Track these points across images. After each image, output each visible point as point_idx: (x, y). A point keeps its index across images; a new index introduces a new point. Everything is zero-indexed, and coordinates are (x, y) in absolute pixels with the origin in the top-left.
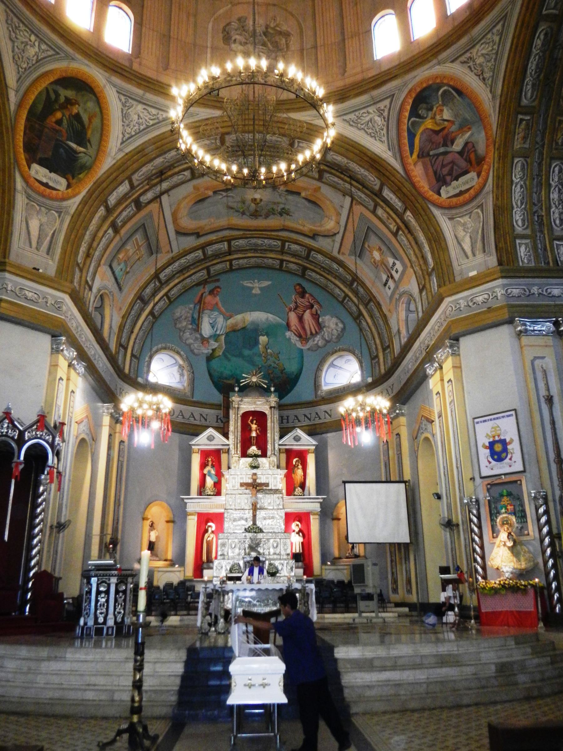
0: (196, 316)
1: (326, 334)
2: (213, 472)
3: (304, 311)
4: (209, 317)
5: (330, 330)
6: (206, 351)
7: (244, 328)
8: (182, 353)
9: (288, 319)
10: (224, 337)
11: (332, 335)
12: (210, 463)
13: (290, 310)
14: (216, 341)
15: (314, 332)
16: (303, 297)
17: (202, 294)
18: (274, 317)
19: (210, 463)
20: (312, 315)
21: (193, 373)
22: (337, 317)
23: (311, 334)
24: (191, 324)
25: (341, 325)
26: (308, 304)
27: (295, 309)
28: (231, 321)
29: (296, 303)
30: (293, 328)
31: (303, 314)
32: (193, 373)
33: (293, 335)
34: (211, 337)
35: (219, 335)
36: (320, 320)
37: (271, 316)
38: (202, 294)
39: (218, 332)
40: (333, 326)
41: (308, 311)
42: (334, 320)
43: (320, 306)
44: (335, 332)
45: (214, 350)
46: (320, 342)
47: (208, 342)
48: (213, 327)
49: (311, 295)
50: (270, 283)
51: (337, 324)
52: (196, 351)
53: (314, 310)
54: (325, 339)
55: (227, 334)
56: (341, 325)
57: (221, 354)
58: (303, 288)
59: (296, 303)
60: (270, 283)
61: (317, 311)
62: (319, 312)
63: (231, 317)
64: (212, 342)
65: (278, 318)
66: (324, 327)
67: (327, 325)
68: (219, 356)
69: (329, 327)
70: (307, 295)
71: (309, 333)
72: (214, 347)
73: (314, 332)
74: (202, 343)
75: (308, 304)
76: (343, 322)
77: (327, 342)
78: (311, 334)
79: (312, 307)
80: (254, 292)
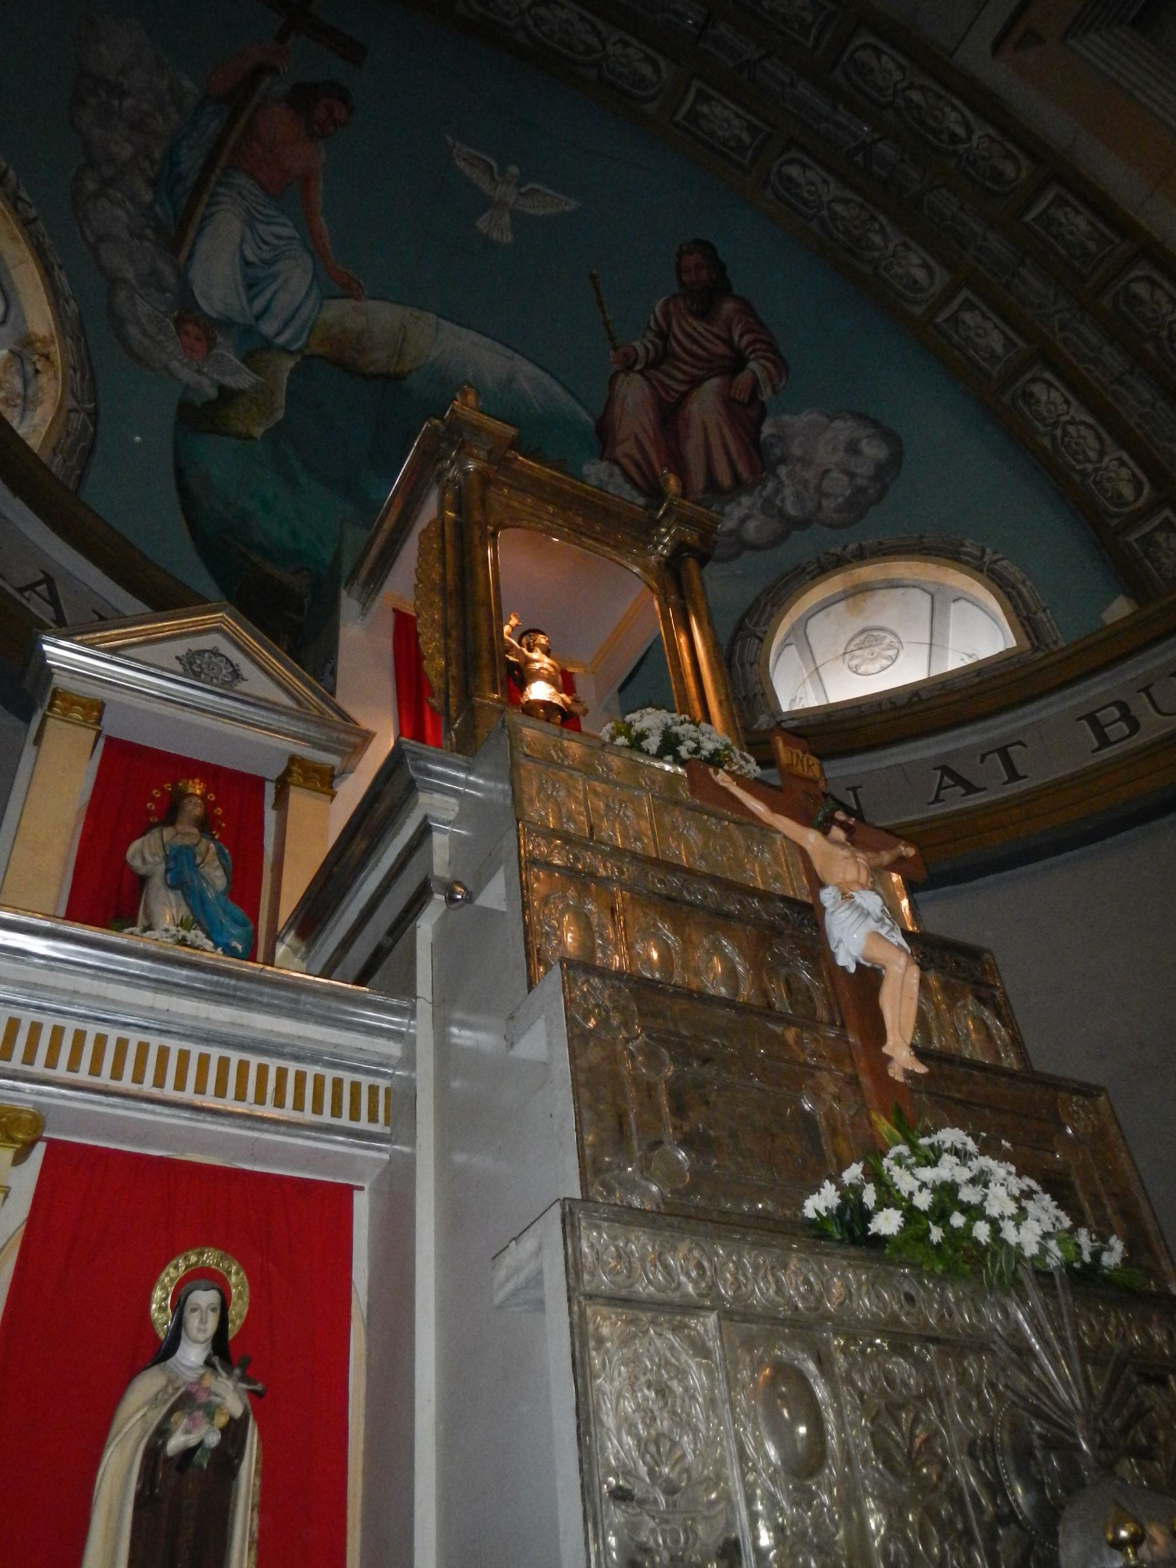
0: (191, 162)
1: (788, 491)
2: (216, 877)
3: (695, 383)
4: (250, 221)
5: (809, 475)
6: (187, 375)
7: (391, 379)
8: (62, 278)
9: (610, 401)
10: (291, 364)
11: (821, 493)
12: (194, 810)
13: (629, 369)
14: (249, 359)
15: (725, 479)
16: (705, 313)
17: (260, 71)
18: (546, 379)
19: (194, 810)
20: (728, 401)
21: (94, 416)
22: (862, 418)
23: (712, 484)
24: (153, 183)
25: (874, 451)
26: (720, 349)
27: (652, 364)
28: (335, 310)
29: (664, 335)
30: (625, 449)
31: (684, 396)
32: (94, 416)
33: (619, 478)
34: (226, 324)
35: (268, 344)
36: (767, 429)
37: (529, 368)
38: (260, 71)
39: (268, 328)
40: (827, 454)
41: (713, 384)
42: (844, 429)
43: (781, 365)
44: (838, 484)
45: (226, 395)
46: (751, 526)
47: (211, 344)
48: (252, 286)
49: (746, 308)
50: (571, 205)
51: (853, 448)
52: (132, 330)
53: (744, 377)
54: (781, 514)
55: (307, 362)
56: (874, 451)
57: (258, 432)
58: (719, 268)
59: (664, 335)
60: (571, 205)
61: (756, 383)
62: (766, 394)
63: (349, 290)
64: (226, 350)
65: (558, 389)
66: (783, 460)
67: (797, 452)
68: (249, 437)
69: (806, 462)
70: (728, 307)
71: (698, 480)
72: (230, 382)
73: (725, 479)
74: (179, 322)
75: (720, 349)
76: (889, 436)
77: (791, 525)
78: (712, 484)
79: (737, 363)
80: (482, 224)
